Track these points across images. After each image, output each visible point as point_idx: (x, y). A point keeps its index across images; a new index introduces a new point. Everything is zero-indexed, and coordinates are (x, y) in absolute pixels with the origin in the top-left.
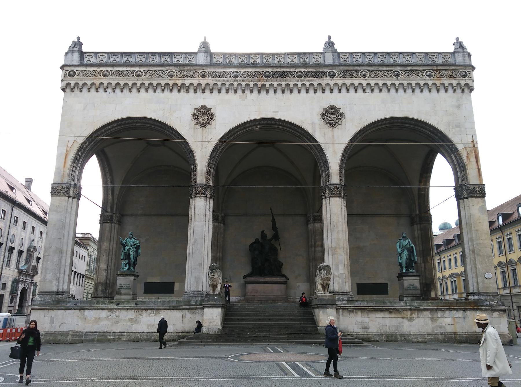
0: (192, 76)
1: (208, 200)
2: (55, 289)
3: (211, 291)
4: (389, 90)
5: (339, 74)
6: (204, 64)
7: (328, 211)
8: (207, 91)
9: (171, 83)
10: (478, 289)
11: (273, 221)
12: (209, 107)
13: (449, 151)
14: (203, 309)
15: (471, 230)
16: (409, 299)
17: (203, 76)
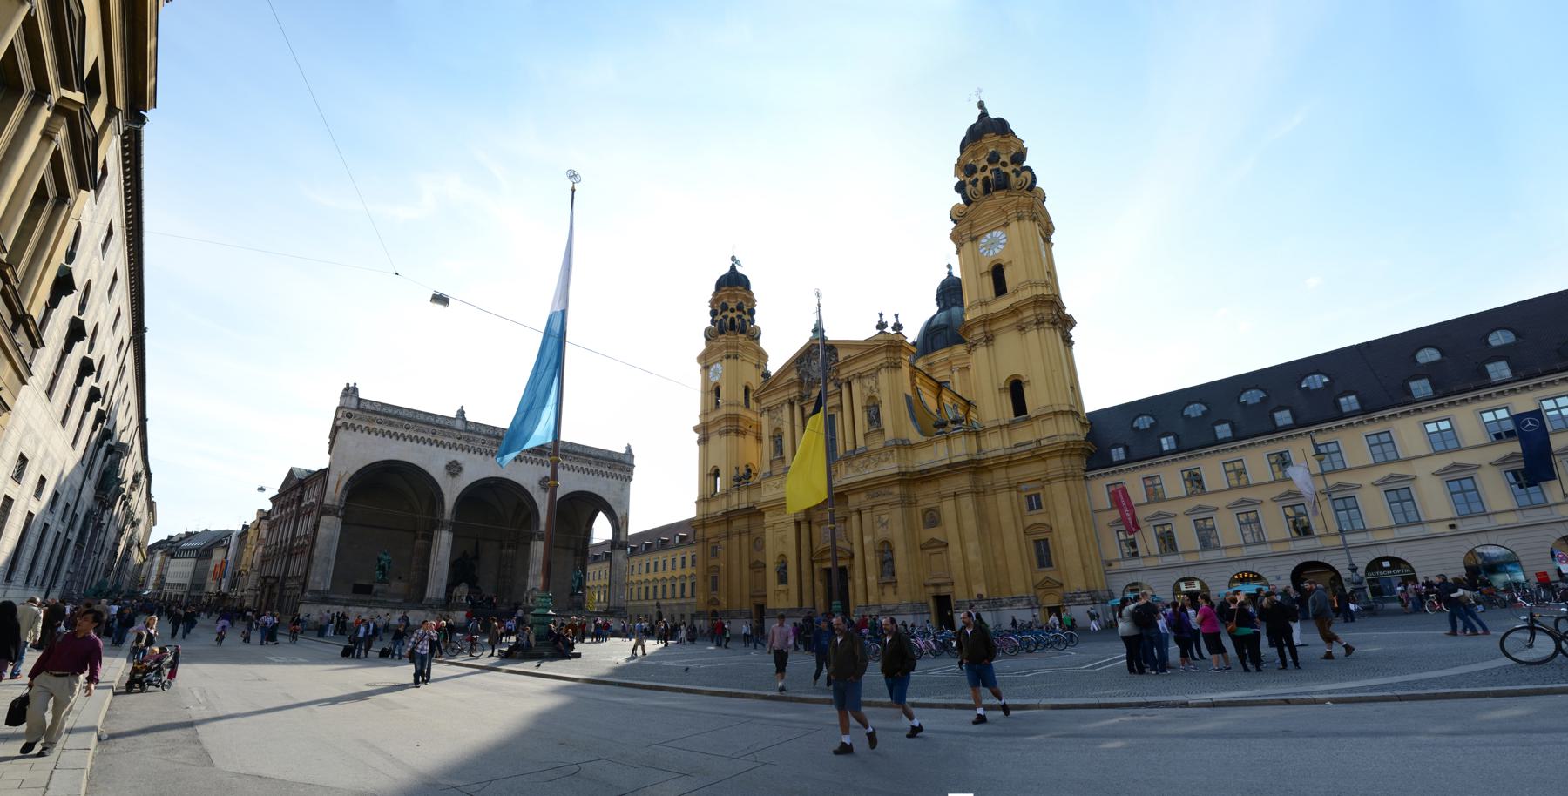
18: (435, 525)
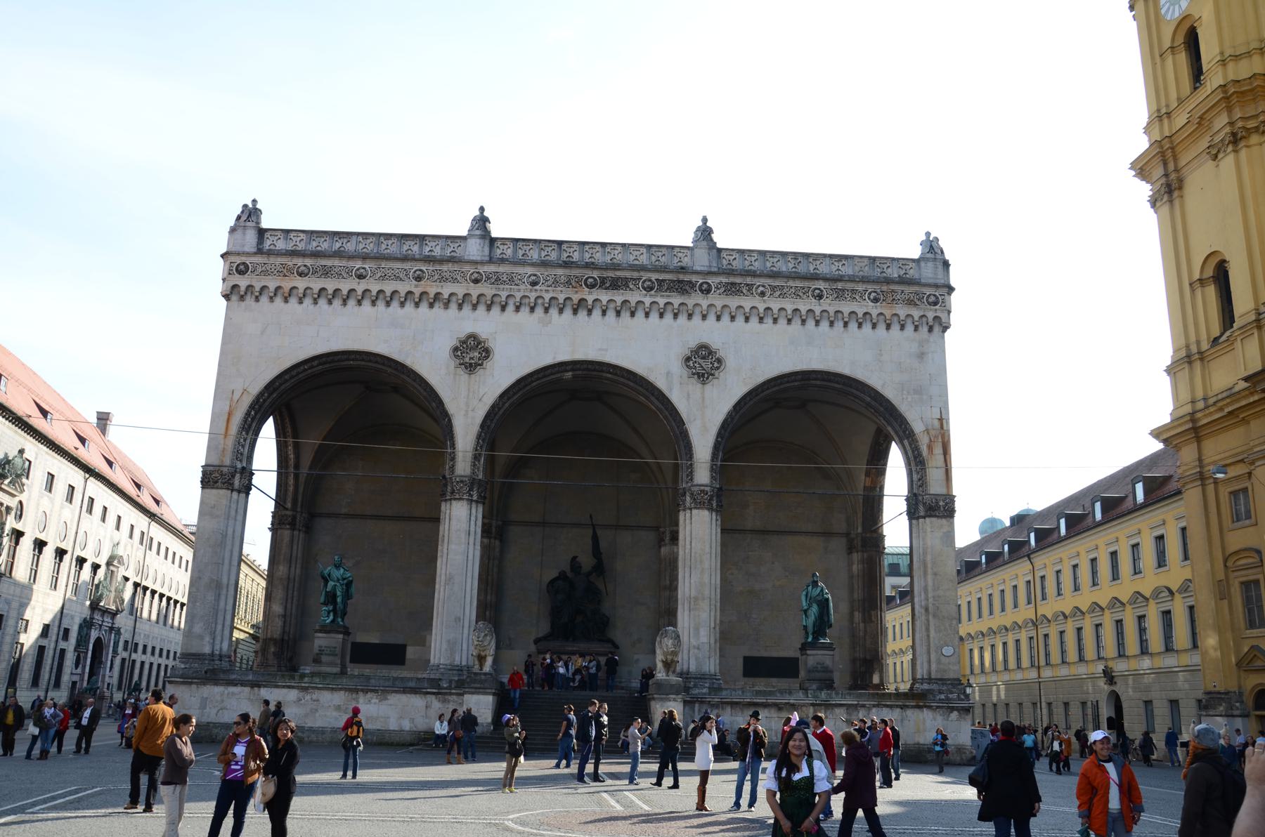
0: (455, 280)
1: (474, 505)
2: (207, 650)
3: (477, 667)
4: (804, 322)
5: (717, 288)
6: (479, 258)
7: (688, 533)
8: (481, 309)
9: (417, 291)
10: (930, 673)
11: (595, 539)
12: (483, 336)
13: (901, 433)
14: (462, 695)
15: (925, 573)
16: (814, 687)
17: (476, 281)
18: (443, 489)
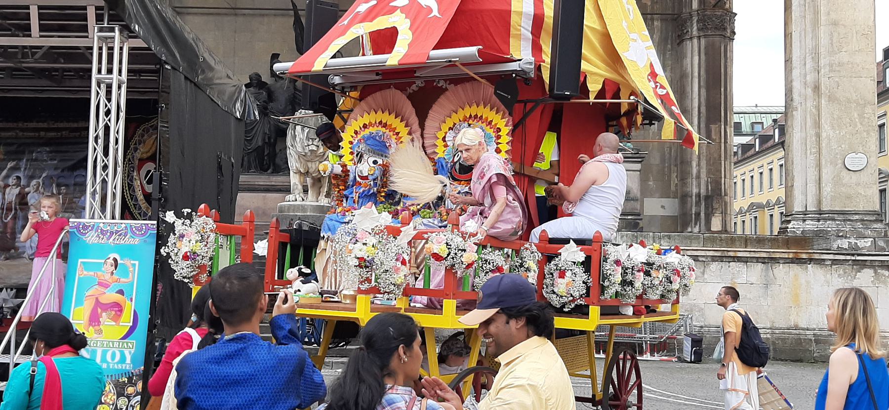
10: (819, 202)
15: (816, 23)
